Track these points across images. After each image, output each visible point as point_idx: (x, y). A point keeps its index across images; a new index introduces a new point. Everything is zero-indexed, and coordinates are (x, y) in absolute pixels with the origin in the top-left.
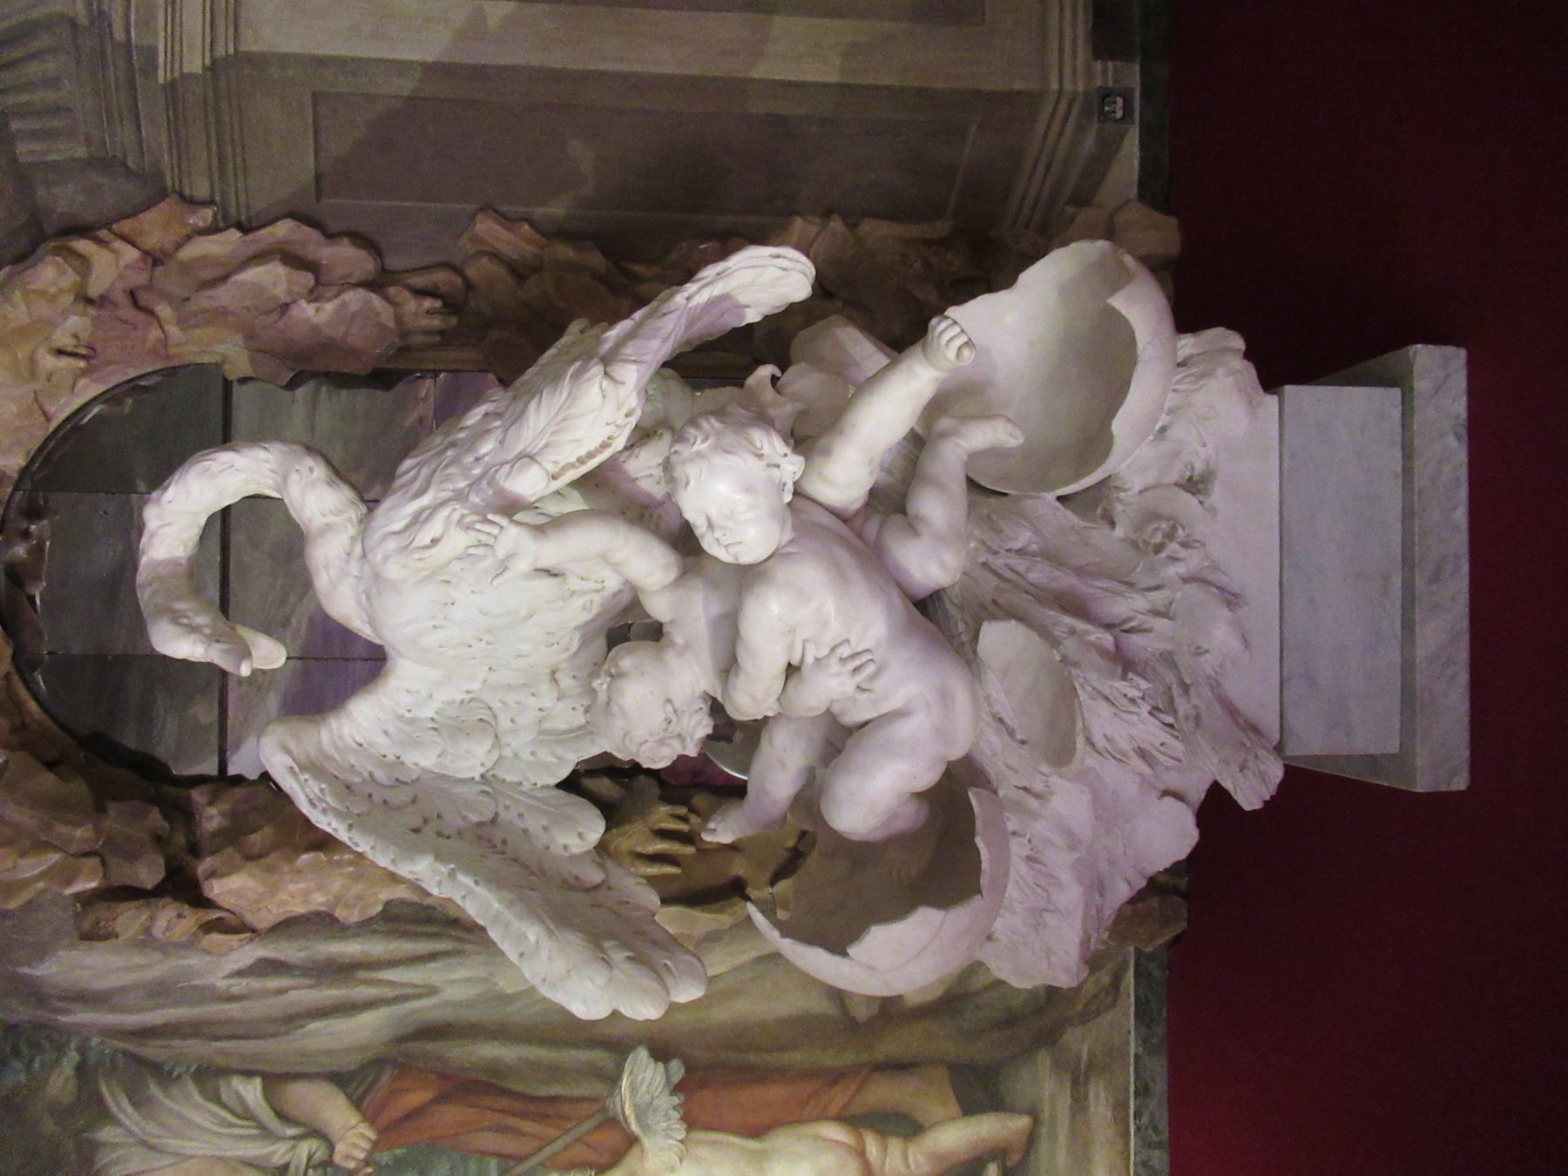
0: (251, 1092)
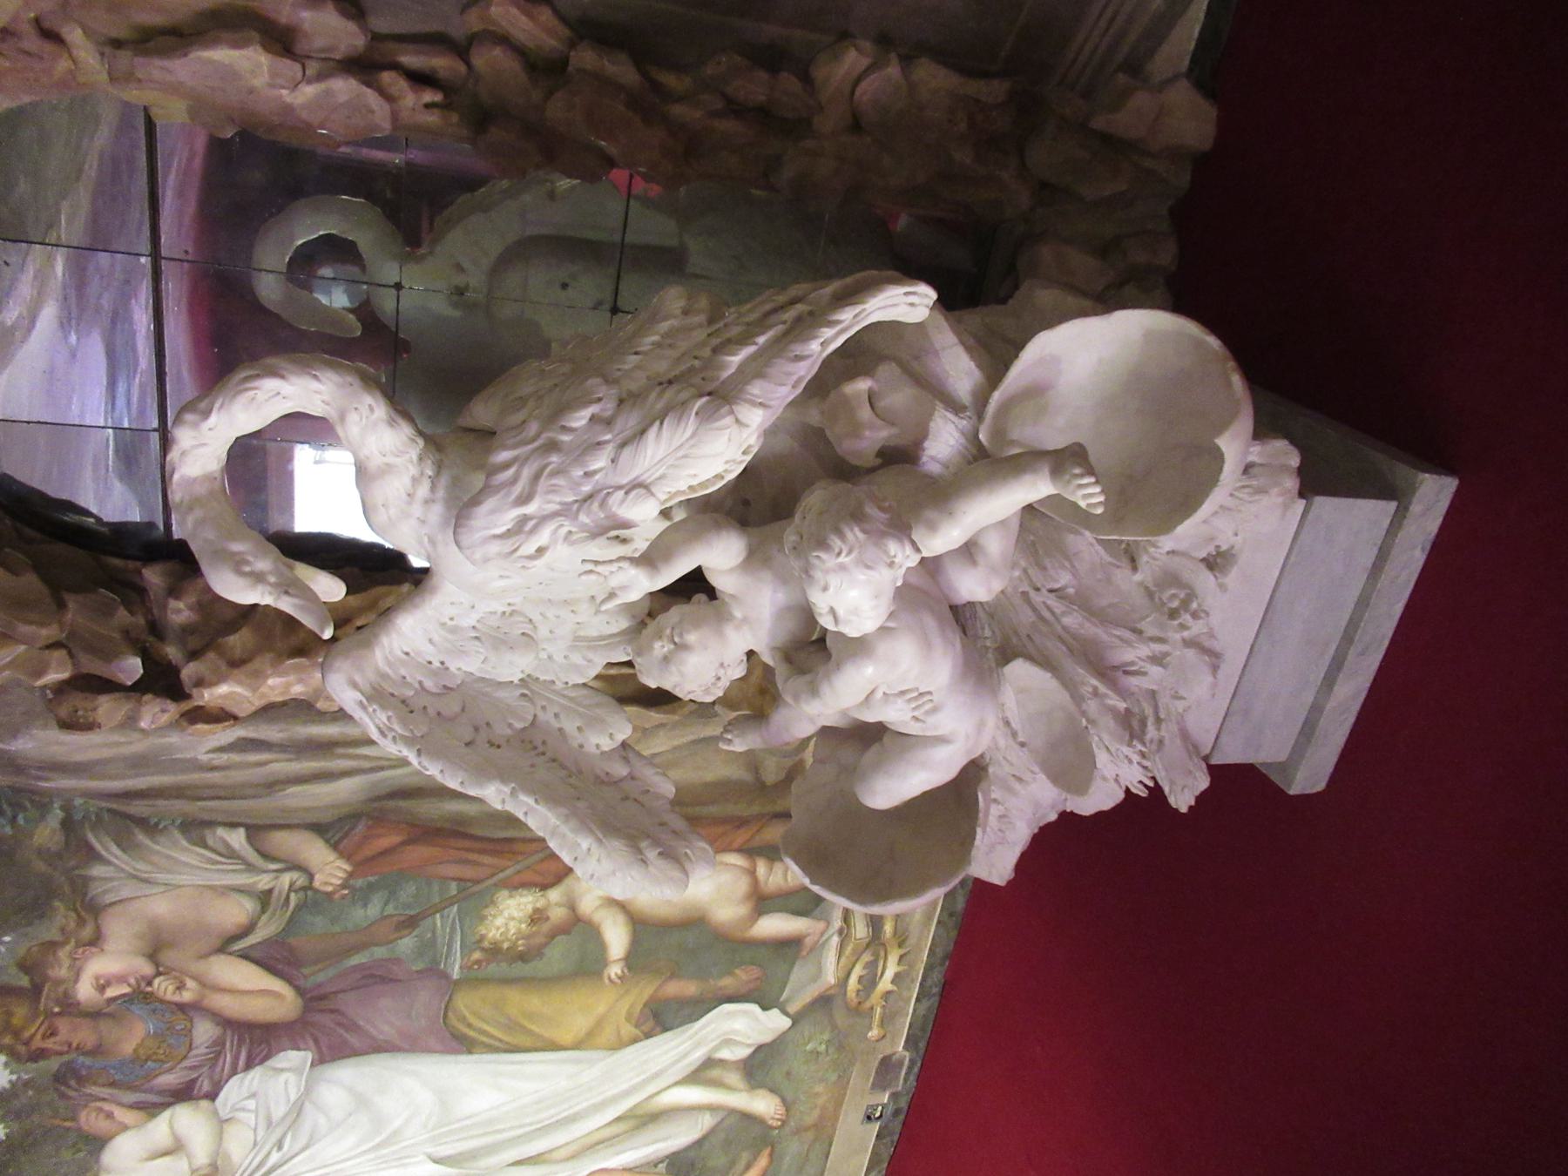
0: (237, 839)
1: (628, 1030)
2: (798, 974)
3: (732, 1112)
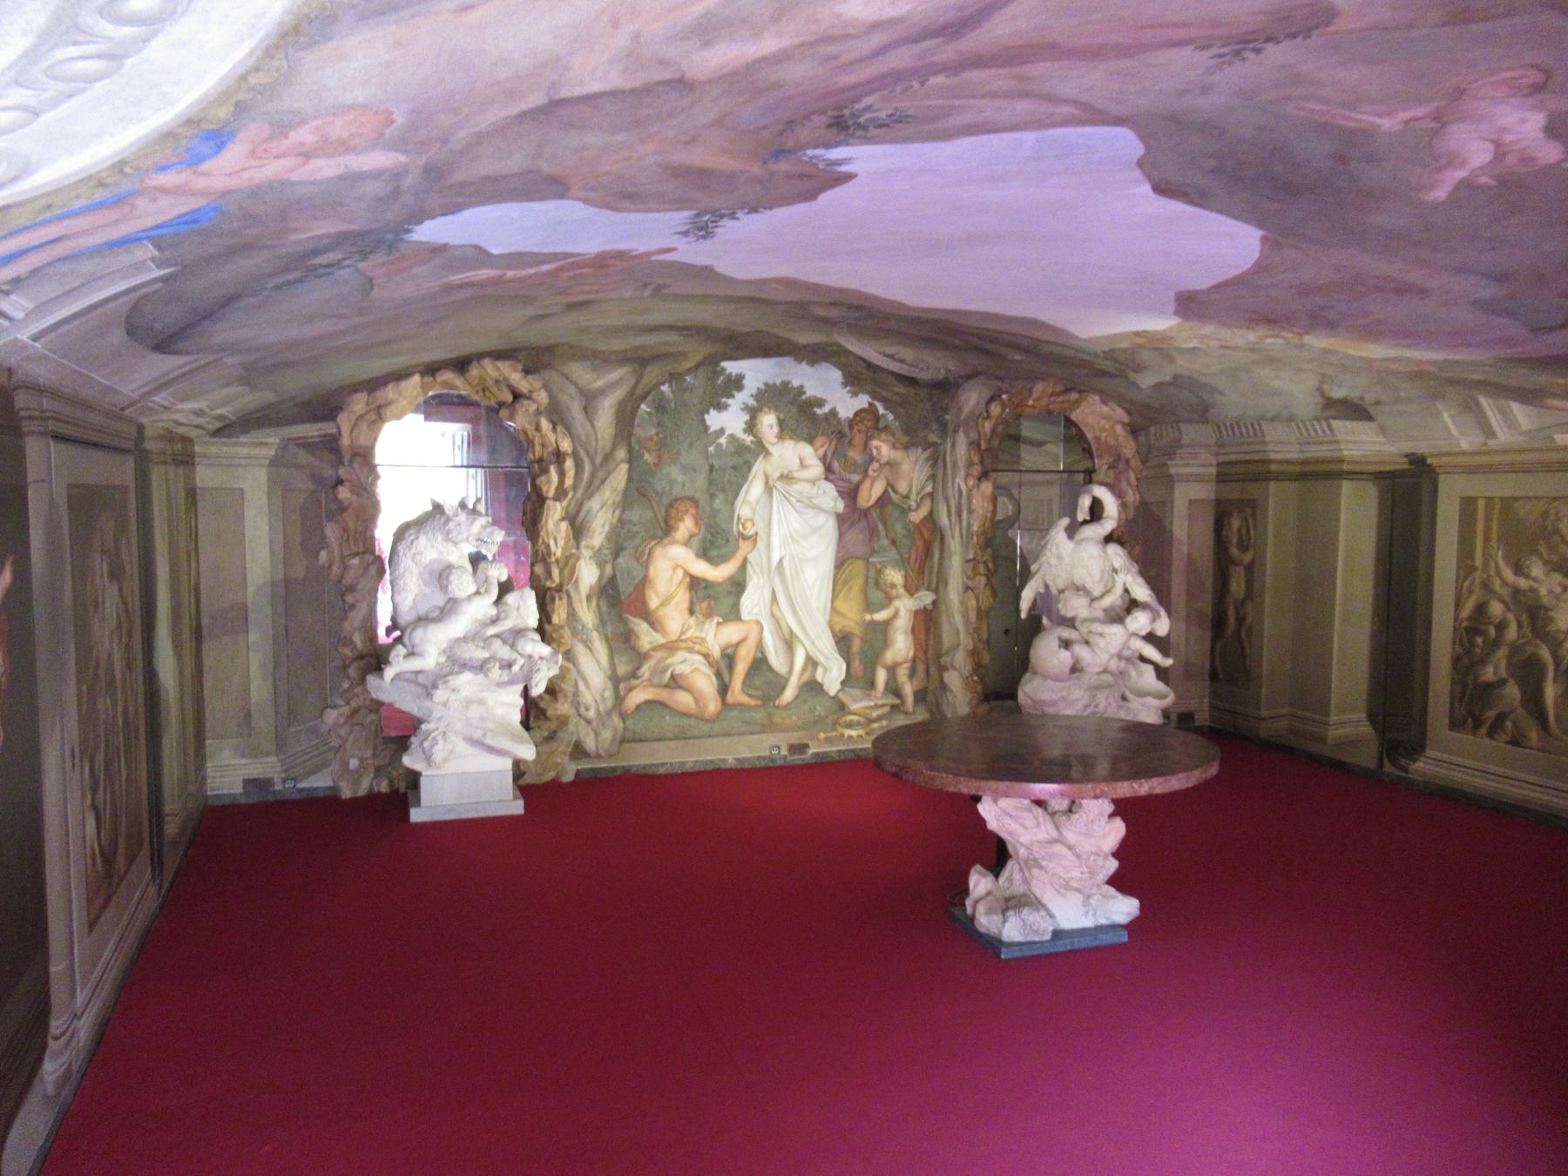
0: (929, 489)
1: (837, 628)
2: (857, 692)
3: (786, 681)
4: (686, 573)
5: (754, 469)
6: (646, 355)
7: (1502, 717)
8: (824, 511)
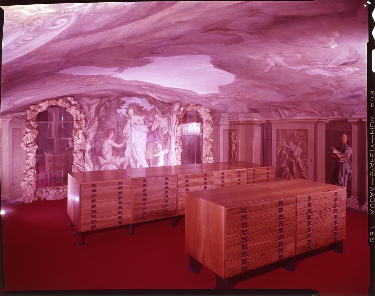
0: (167, 127)
1: (147, 158)
4: (112, 146)
5: (128, 122)
6: (103, 96)
7: (286, 175)
8: (144, 131)
